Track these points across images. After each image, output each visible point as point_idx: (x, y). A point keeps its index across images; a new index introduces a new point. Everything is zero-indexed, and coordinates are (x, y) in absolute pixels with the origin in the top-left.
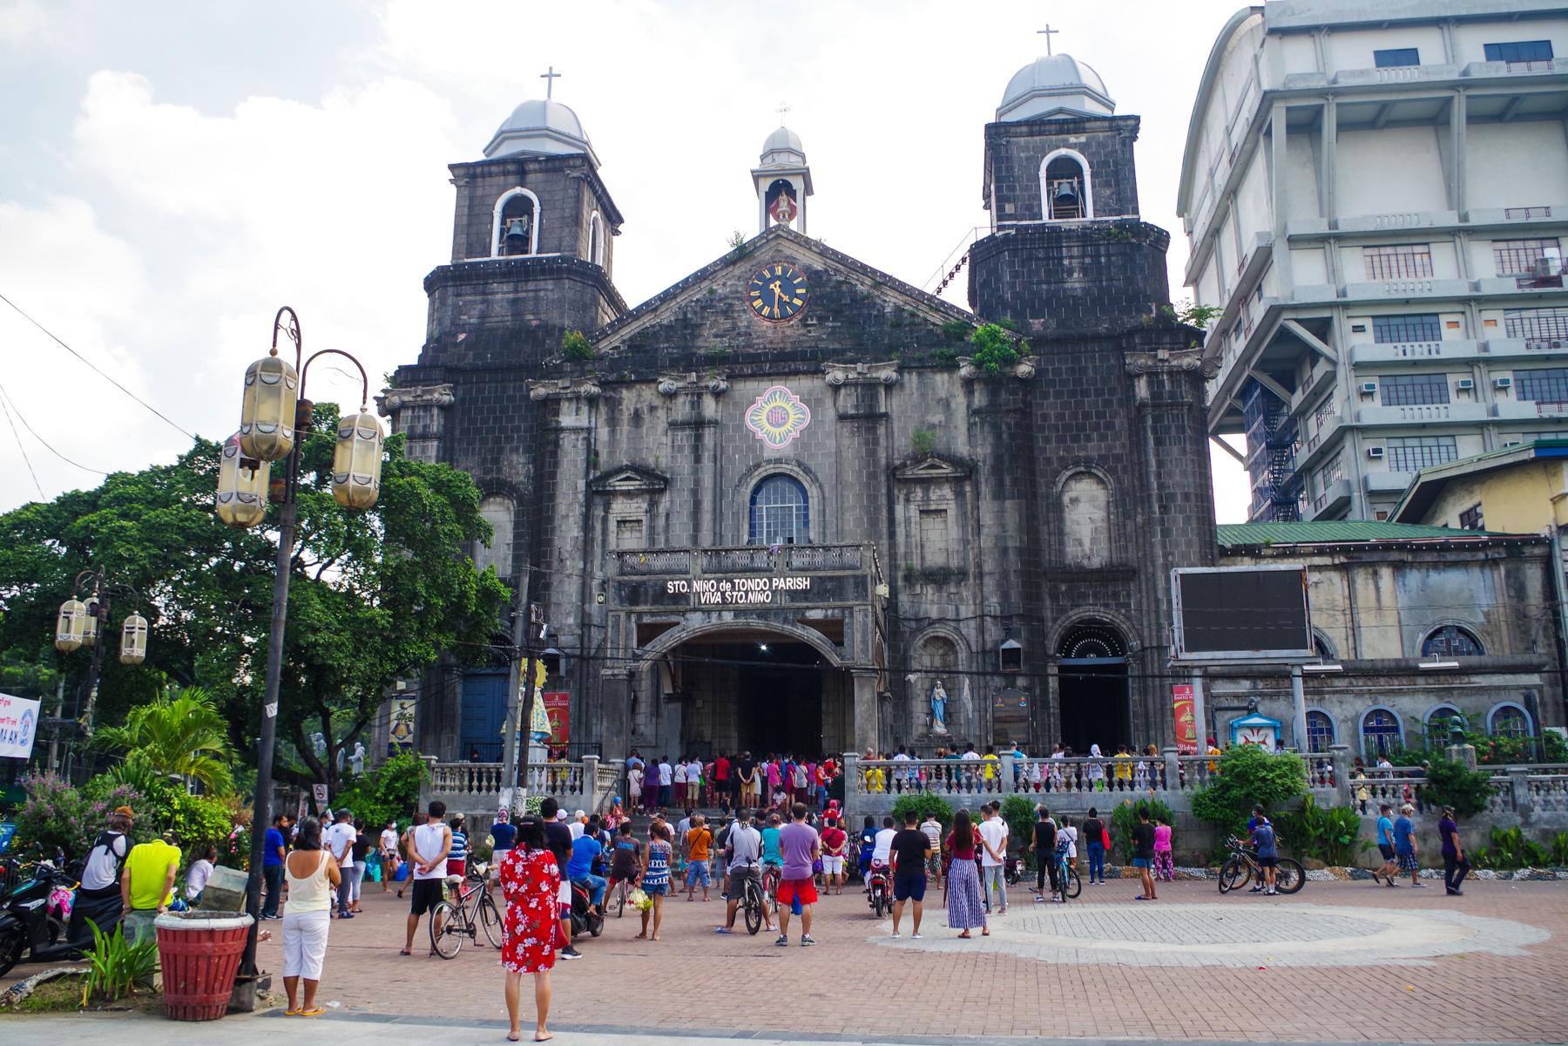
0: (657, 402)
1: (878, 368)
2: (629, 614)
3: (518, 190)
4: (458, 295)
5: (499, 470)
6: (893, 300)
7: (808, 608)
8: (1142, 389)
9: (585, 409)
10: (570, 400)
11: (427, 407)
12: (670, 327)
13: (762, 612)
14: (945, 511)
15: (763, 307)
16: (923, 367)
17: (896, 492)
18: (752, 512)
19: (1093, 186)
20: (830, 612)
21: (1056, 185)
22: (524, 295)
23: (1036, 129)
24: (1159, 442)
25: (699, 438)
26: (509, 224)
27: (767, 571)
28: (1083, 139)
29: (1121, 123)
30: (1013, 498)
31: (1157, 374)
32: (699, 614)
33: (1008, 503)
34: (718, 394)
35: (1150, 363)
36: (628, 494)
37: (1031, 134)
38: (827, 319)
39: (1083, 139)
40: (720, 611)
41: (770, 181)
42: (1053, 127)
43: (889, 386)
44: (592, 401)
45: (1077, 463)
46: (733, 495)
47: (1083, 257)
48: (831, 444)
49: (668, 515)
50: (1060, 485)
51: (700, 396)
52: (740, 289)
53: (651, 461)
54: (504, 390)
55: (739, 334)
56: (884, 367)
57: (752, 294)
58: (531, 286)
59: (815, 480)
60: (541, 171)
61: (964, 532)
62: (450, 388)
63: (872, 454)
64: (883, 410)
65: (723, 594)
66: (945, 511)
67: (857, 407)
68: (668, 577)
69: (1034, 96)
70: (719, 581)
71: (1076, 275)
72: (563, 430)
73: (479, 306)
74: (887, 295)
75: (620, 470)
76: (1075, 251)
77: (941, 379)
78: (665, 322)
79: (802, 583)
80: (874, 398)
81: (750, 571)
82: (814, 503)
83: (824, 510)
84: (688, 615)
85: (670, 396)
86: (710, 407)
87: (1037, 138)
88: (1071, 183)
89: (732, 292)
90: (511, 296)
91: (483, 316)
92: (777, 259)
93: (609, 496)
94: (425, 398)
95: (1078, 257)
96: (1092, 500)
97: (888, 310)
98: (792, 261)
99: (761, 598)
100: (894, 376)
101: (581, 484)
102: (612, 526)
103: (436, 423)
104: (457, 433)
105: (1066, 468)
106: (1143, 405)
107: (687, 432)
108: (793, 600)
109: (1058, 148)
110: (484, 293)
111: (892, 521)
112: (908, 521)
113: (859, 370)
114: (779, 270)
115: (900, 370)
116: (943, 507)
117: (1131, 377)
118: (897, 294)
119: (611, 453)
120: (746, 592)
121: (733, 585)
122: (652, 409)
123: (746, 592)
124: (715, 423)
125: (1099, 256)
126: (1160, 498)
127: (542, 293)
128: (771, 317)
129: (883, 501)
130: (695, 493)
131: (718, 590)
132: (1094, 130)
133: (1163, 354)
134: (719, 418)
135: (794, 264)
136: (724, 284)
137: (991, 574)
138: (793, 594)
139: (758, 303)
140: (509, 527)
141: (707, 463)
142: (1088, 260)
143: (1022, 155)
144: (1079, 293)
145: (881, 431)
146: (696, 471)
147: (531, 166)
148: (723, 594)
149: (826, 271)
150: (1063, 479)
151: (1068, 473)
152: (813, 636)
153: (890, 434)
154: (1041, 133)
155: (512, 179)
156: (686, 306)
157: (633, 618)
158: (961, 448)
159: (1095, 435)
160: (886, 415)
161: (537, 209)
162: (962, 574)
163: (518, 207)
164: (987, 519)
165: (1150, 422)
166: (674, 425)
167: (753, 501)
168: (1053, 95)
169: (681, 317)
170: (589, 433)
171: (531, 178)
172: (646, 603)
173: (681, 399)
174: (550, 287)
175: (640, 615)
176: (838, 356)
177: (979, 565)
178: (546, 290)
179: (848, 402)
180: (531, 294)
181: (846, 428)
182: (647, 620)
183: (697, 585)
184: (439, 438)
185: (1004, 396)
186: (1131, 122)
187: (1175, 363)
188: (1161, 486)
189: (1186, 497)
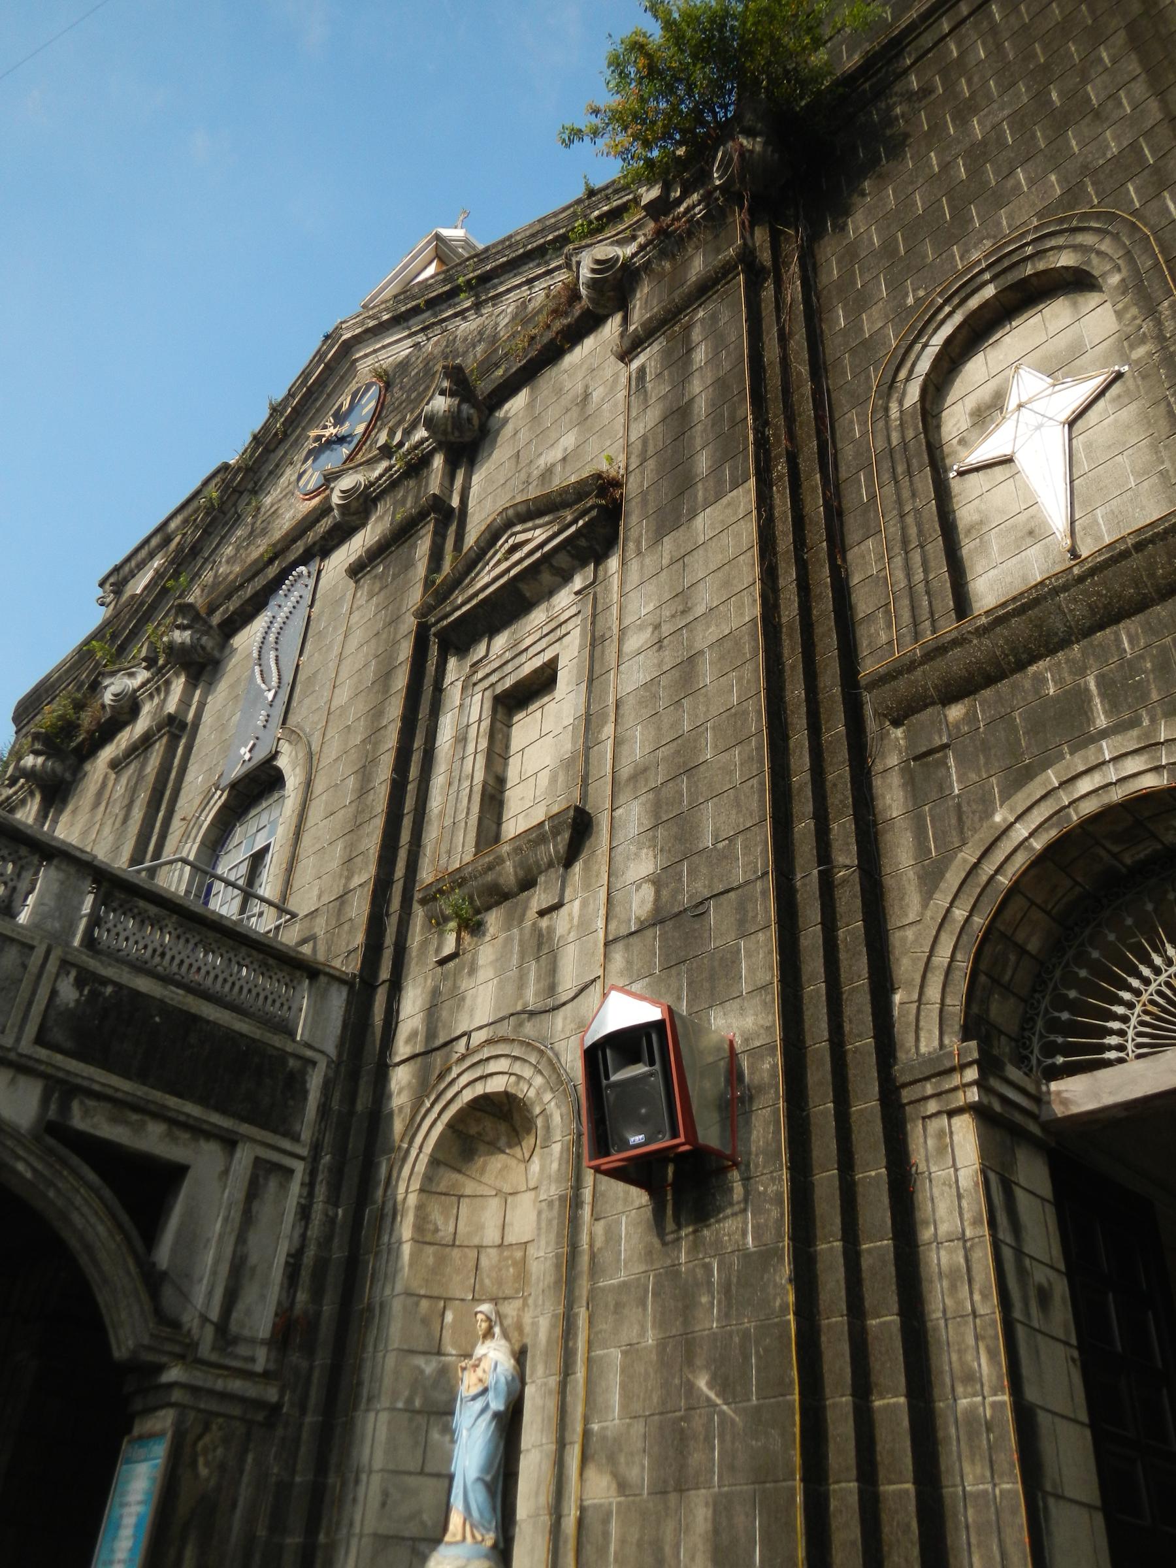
150: (924, 366)
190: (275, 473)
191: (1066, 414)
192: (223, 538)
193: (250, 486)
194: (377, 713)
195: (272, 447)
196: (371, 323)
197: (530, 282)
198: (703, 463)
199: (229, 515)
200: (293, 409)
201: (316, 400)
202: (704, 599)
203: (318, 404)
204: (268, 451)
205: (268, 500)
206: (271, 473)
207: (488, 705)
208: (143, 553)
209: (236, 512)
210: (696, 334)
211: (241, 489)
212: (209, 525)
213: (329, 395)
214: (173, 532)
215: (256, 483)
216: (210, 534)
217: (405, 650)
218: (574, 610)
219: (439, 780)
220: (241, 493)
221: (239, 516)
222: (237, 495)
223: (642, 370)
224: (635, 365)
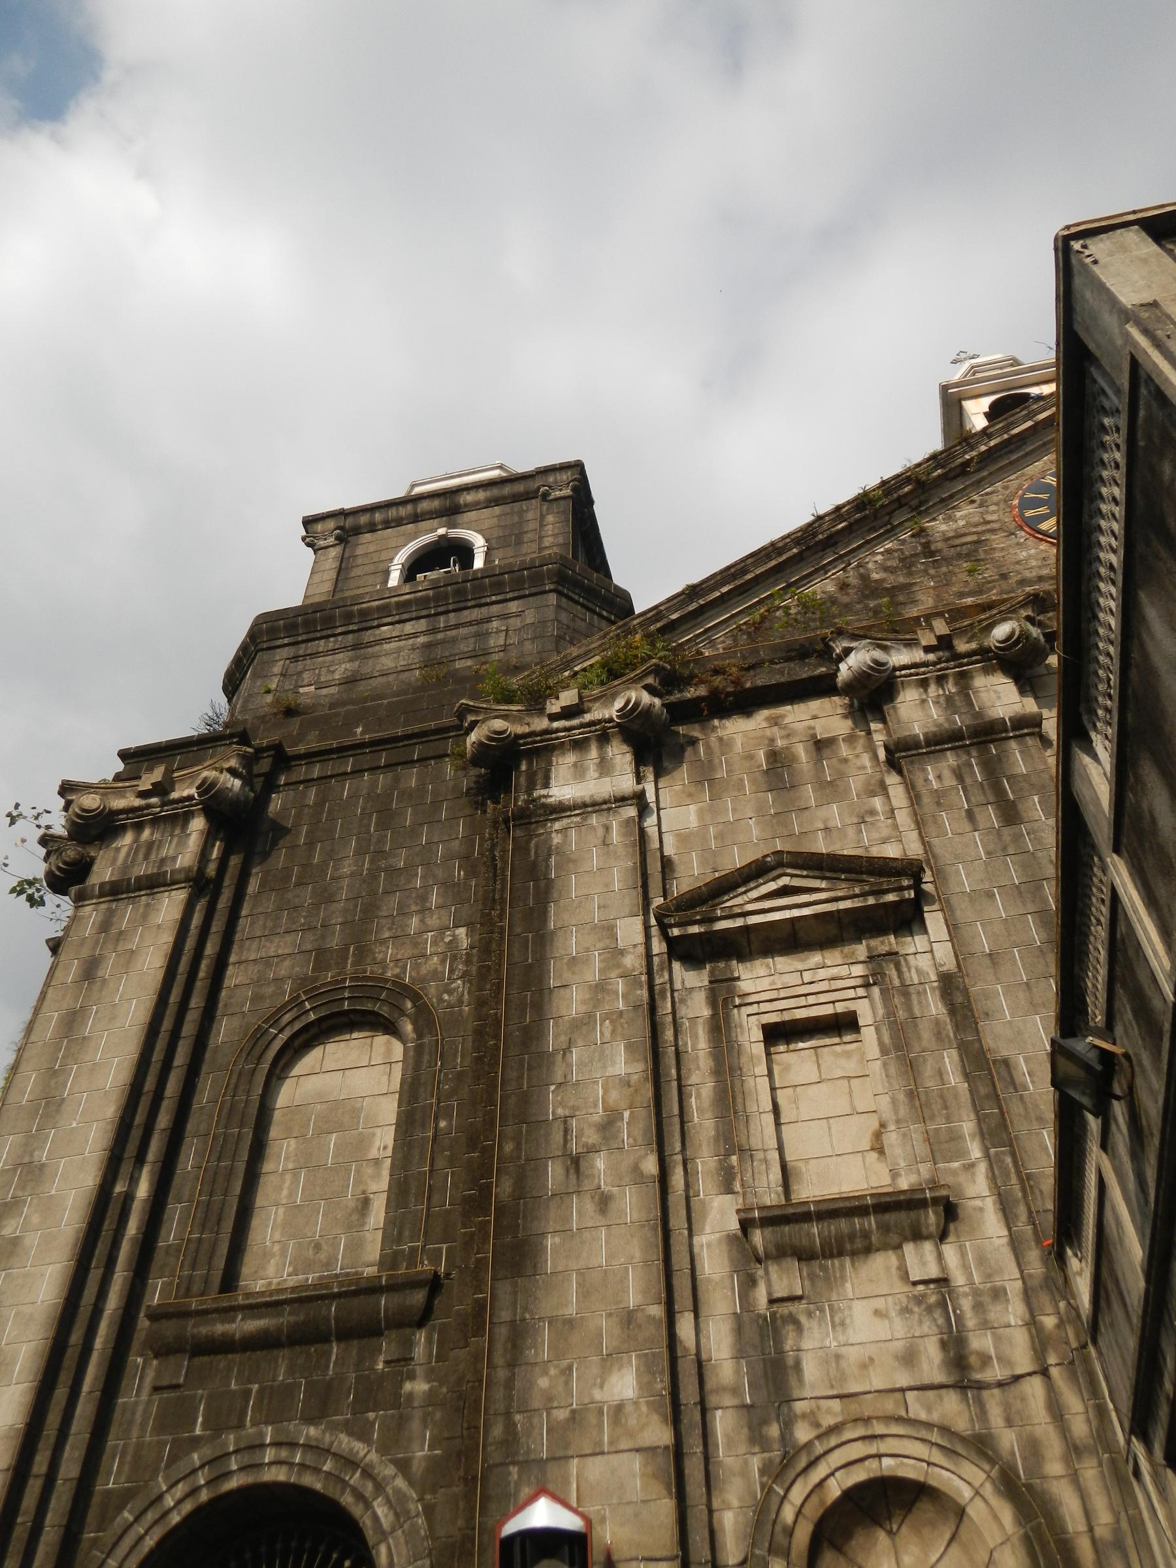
3: (442, 531)
4: (295, 659)
5: (363, 952)
9: (620, 755)
10: (579, 745)
22: (453, 633)
25: (994, 770)
41: (985, 403)
49: (949, 984)
51: (964, 678)
52: (989, 518)
54: (397, 780)
75: (757, 871)
89: (968, 524)
90: (422, 640)
91: (351, 681)
102: (750, 1036)
104: (253, 886)
107: (951, 759)
122: (821, 746)
127: (495, 624)
140: (389, 1110)
147: (469, 498)
169: (853, 580)
190: (947, 503)
192: (868, 542)
193: (914, 503)
195: (951, 475)
199: (879, 522)
200: (990, 449)
201: (1011, 452)
203: (1014, 457)
204: (947, 478)
205: (939, 526)
206: (942, 500)
208: (403, 511)
209: (889, 523)
211: (903, 501)
212: (857, 521)
213: (1027, 455)
214: (466, 505)
215: (921, 504)
216: (851, 532)
220: (901, 506)
221: (893, 528)
222: (896, 505)
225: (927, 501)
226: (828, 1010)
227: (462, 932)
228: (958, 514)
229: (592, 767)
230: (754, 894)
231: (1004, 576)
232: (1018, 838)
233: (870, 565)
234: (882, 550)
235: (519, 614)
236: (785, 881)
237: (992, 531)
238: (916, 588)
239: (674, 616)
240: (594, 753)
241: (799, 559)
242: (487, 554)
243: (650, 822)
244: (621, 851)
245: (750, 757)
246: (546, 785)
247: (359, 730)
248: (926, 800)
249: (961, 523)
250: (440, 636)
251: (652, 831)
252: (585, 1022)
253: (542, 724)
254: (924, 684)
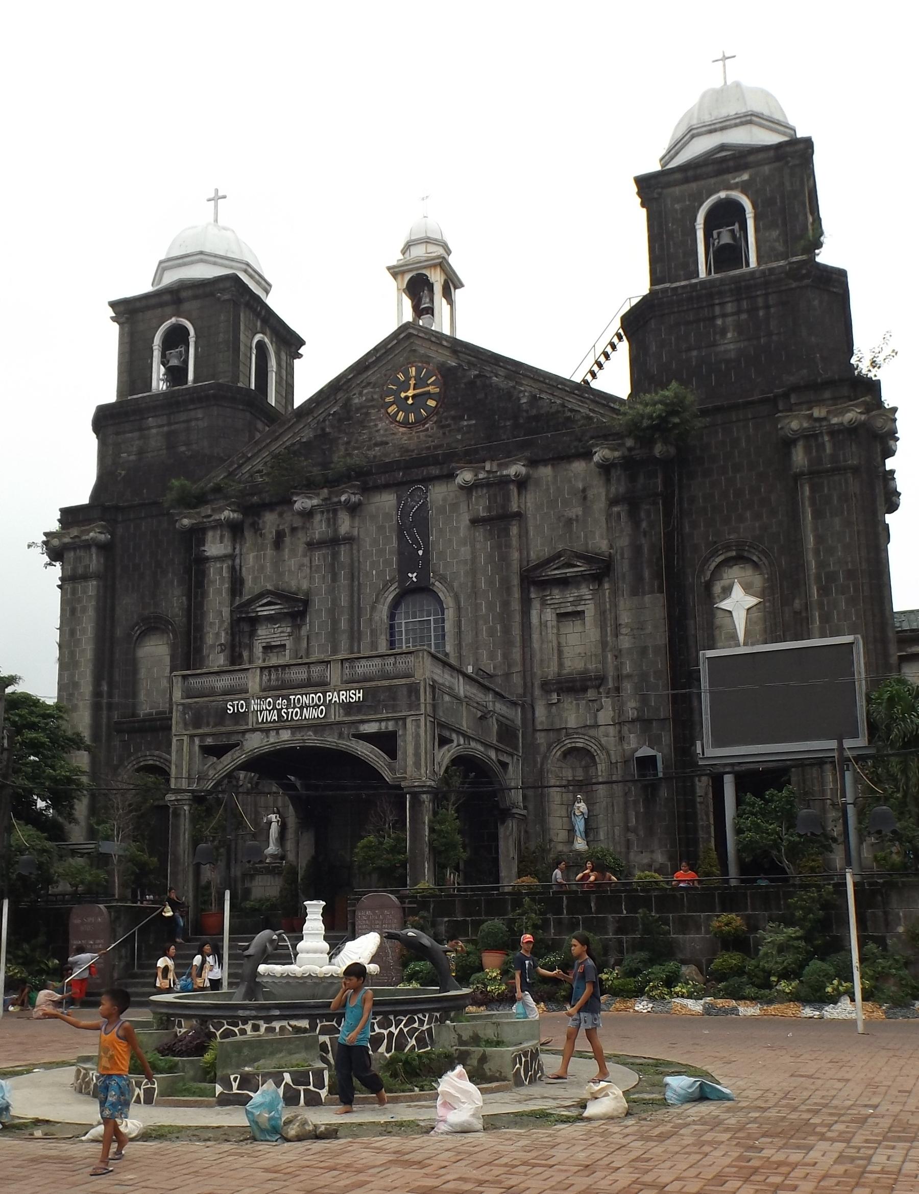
0: (298, 522)
1: (506, 465)
2: (192, 737)
3: (173, 320)
6: (528, 388)
7: (363, 722)
8: (799, 457)
9: (227, 535)
10: (214, 528)
11: (87, 546)
12: (307, 445)
13: (317, 726)
14: (583, 612)
15: (397, 413)
16: (561, 458)
17: (533, 596)
18: (392, 627)
19: (757, 230)
20: (383, 724)
21: (715, 236)
22: (177, 426)
23: (690, 173)
24: (818, 514)
25: (335, 555)
26: (168, 356)
27: (322, 685)
28: (745, 177)
29: (788, 149)
30: (652, 592)
31: (815, 436)
32: (258, 735)
33: (647, 598)
34: (353, 509)
35: (805, 425)
36: (271, 619)
37: (686, 181)
38: (462, 418)
39: (745, 177)
40: (277, 730)
42: (710, 169)
43: (522, 483)
44: (235, 530)
45: (728, 548)
46: (371, 615)
47: (738, 312)
48: (465, 552)
50: (708, 574)
51: (335, 512)
52: (375, 396)
53: (293, 585)
55: (376, 445)
56: (514, 463)
57: (387, 400)
58: (183, 417)
59: (450, 588)
60: (196, 297)
61: (603, 634)
62: (102, 526)
63: (504, 558)
64: (515, 508)
65: (279, 711)
66: (583, 612)
67: (489, 509)
68: (228, 697)
69: (693, 137)
70: (278, 697)
71: (729, 335)
72: (207, 559)
73: (137, 442)
74: (522, 385)
75: (261, 595)
76: (730, 308)
77: (579, 466)
78: (304, 440)
79: (357, 695)
80: (507, 498)
81: (309, 685)
82: (450, 614)
83: (460, 621)
84: (247, 736)
85: (308, 514)
86: (345, 525)
87: (694, 186)
88: (732, 231)
90: (165, 429)
92: (412, 359)
93: (255, 622)
94: (84, 538)
95: (733, 314)
96: (748, 589)
97: (524, 400)
98: (426, 359)
99: (315, 713)
100: (523, 470)
101: (226, 612)
103: (94, 561)
105: (715, 553)
106: (797, 477)
108: (348, 714)
109: (718, 192)
110: (141, 429)
111: (526, 625)
112: (543, 624)
113: (488, 468)
114: (413, 371)
115: (533, 463)
116: (579, 608)
117: (788, 444)
118: (531, 383)
119: (255, 579)
120: (301, 708)
121: (289, 700)
123: (301, 708)
124: (350, 540)
125: (757, 309)
126: (818, 578)
127: (193, 424)
128: (405, 423)
129: (516, 606)
130: (332, 612)
131: (274, 708)
132: (759, 164)
133: (817, 412)
134: (356, 533)
135: (428, 363)
136: (361, 394)
137: (629, 676)
138: (348, 707)
139: (392, 409)
141: (343, 581)
142: (744, 316)
143: (677, 206)
144: (733, 355)
145: (514, 530)
146: (332, 591)
148: (279, 711)
149: (460, 365)
150: (712, 567)
151: (719, 560)
152: (364, 750)
153: (523, 534)
154: (696, 178)
155: (169, 310)
156: (324, 421)
157: (197, 741)
158: (600, 543)
159: (748, 514)
160: (519, 515)
161: (192, 340)
162: (600, 680)
163: (176, 338)
164: (625, 618)
165: (807, 492)
166: (311, 546)
167: (392, 616)
168: (715, 131)
169: (319, 432)
170: (234, 560)
171: (186, 306)
172: (208, 725)
173: (318, 517)
174: (200, 416)
175: (202, 736)
176: (471, 458)
177: (618, 668)
178: (197, 419)
179: (481, 506)
180: (183, 426)
181: (480, 534)
182: (209, 741)
183: (254, 706)
184: (98, 577)
185: (641, 480)
186: (802, 146)
187: (835, 420)
188: (821, 565)
189: (850, 574)
191: (747, 607)
192: (326, 409)
194: (506, 604)
196: (433, 339)
197: (541, 391)
198: (647, 574)
202: (649, 629)
207: (554, 616)
210: (643, 515)
215: (349, 387)
217: (516, 581)
218: (590, 597)
219: (535, 636)
223: (619, 514)
224: (616, 509)
225: (351, 386)
226: (279, 643)
227: (184, 598)
228: (365, 391)
229: (218, 538)
230: (260, 603)
231: (370, 439)
232: (334, 588)
233: (327, 422)
234: (332, 412)
235: (202, 419)
236: (269, 599)
237: (373, 407)
238: (340, 441)
239: (249, 455)
240: (219, 532)
241: (297, 422)
242: (196, 343)
243: (237, 561)
244: (227, 580)
245: (271, 532)
246: (204, 545)
247: (145, 491)
248: (313, 569)
249: (364, 398)
250: (173, 427)
251: (238, 568)
252: (212, 647)
253: (201, 520)
254: (322, 512)
